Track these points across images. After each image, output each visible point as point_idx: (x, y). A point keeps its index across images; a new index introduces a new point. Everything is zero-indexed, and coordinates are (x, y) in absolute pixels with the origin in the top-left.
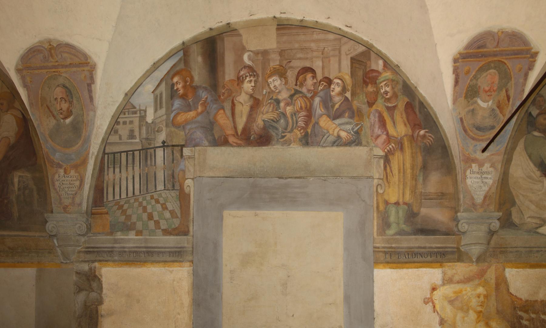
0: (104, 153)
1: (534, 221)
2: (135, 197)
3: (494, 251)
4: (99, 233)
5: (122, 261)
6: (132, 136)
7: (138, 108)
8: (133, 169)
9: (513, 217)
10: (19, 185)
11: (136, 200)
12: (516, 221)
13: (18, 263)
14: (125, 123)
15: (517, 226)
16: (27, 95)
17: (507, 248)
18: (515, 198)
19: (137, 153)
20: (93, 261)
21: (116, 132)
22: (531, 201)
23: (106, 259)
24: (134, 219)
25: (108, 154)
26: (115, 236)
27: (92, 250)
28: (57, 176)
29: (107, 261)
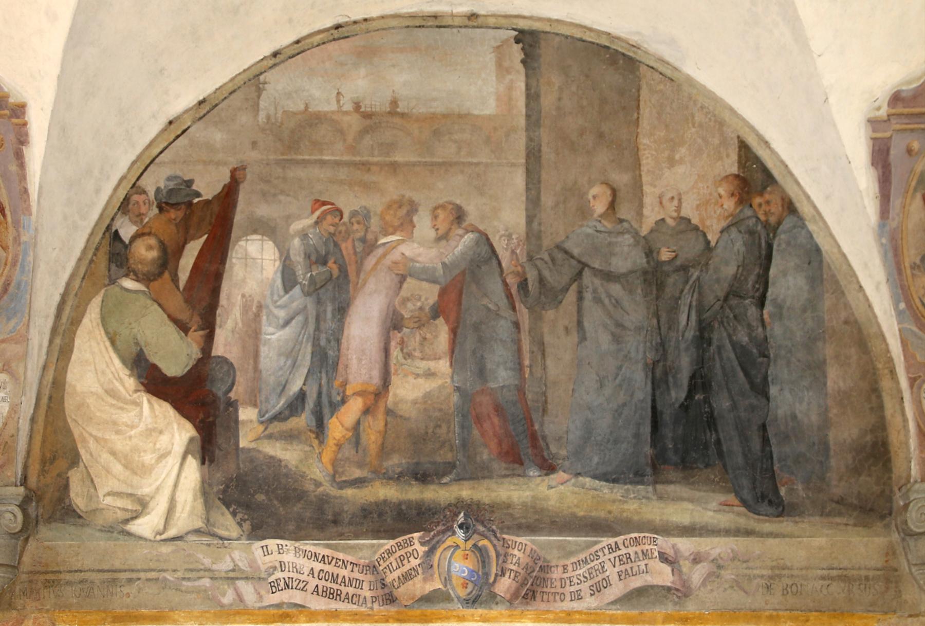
1: (120, 503)
3: (31, 581)
9: (72, 495)
12: (79, 504)
15: (80, 517)
17: (60, 572)
18: (79, 446)
22: (113, 453)
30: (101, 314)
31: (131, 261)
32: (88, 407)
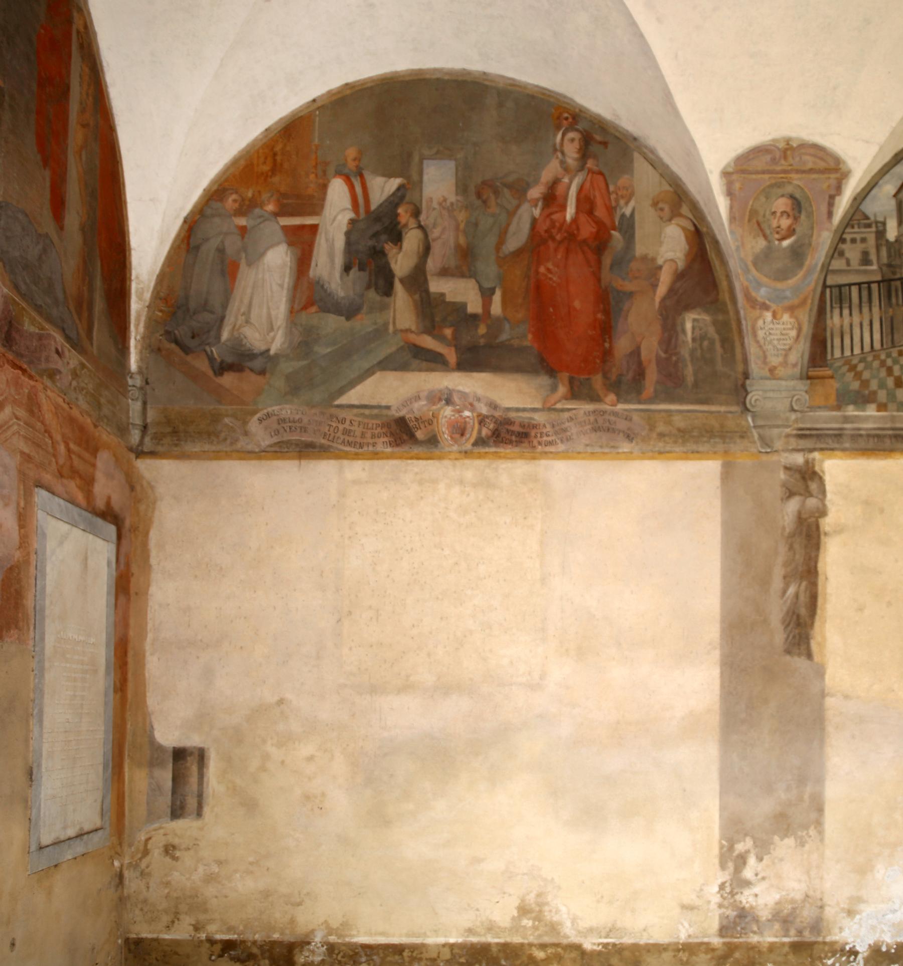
0: (825, 286)
2: (874, 353)
4: (819, 407)
5: (857, 450)
6: (865, 259)
7: (872, 218)
8: (870, 310)
10: (693, 333)
11: (876, 357)
13: (693, 452)
14: (853, 241)
16: (728, 206)
19: (874, 287)
20: (811, 450)
21: (842, 254)
23: (832, 447)
24: (874, 385)
25: (830, 287)
26: (845, 411)
27: (808, 432)
28: (760, 323)
29: (832, 449)
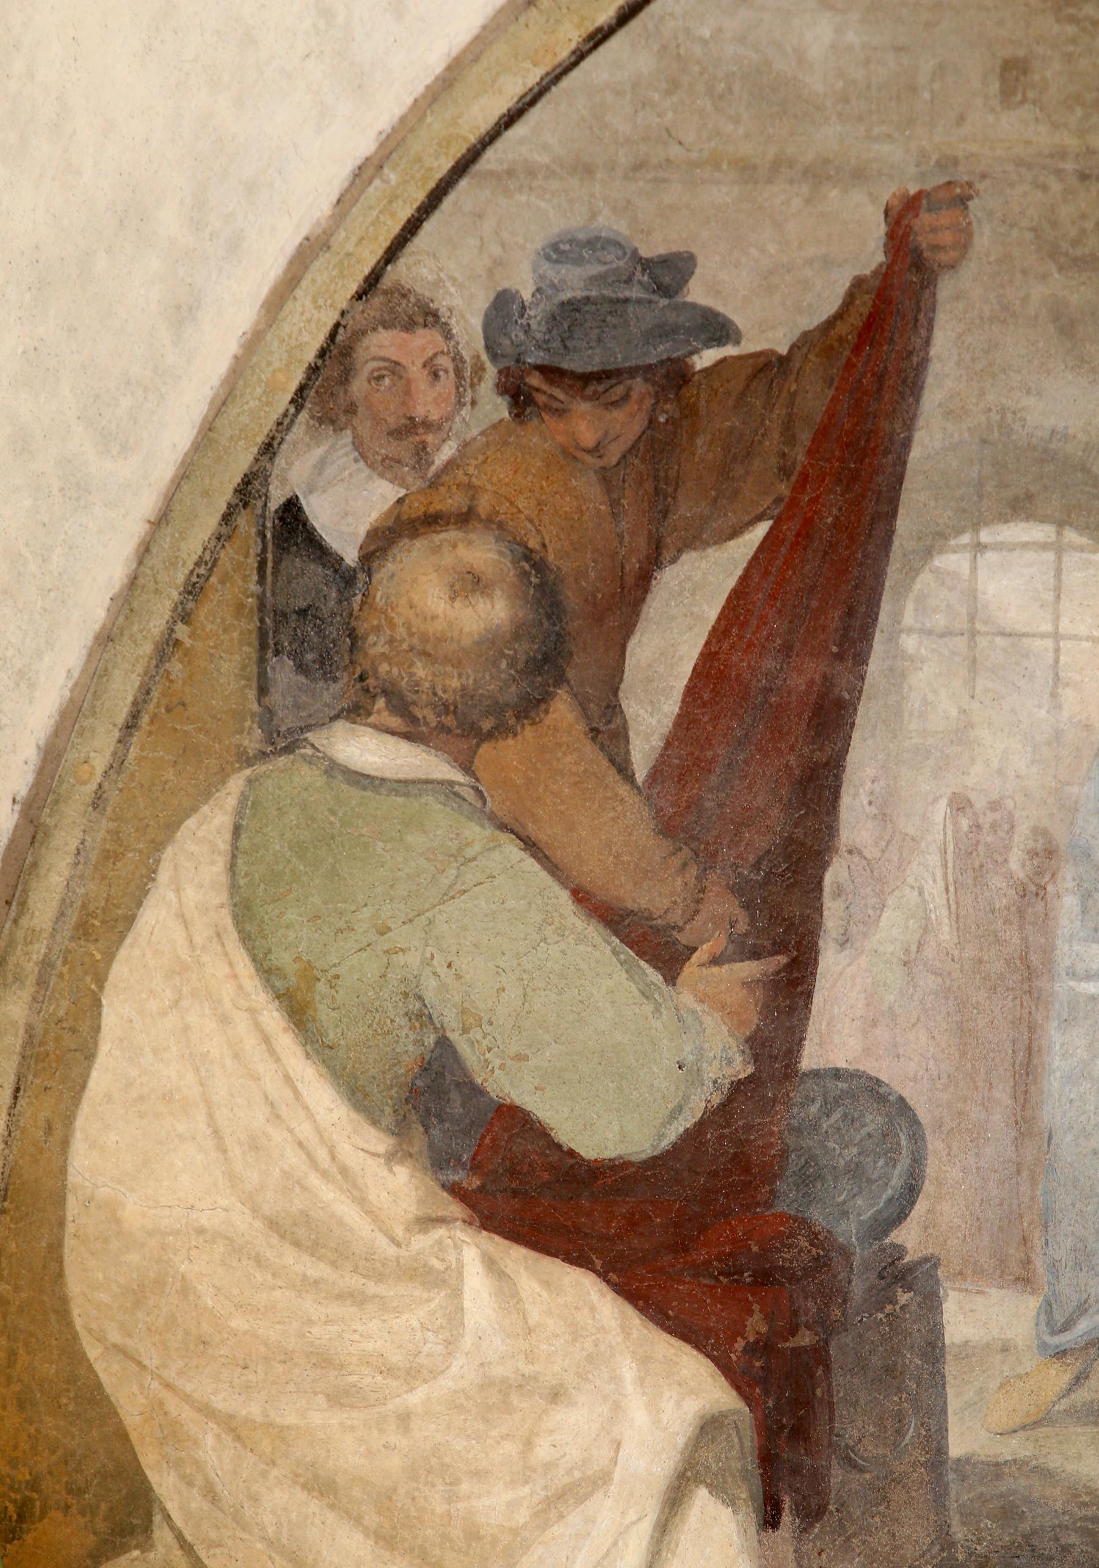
30: (233, 888)
31: (376, 646)
32: (186, 1290)
